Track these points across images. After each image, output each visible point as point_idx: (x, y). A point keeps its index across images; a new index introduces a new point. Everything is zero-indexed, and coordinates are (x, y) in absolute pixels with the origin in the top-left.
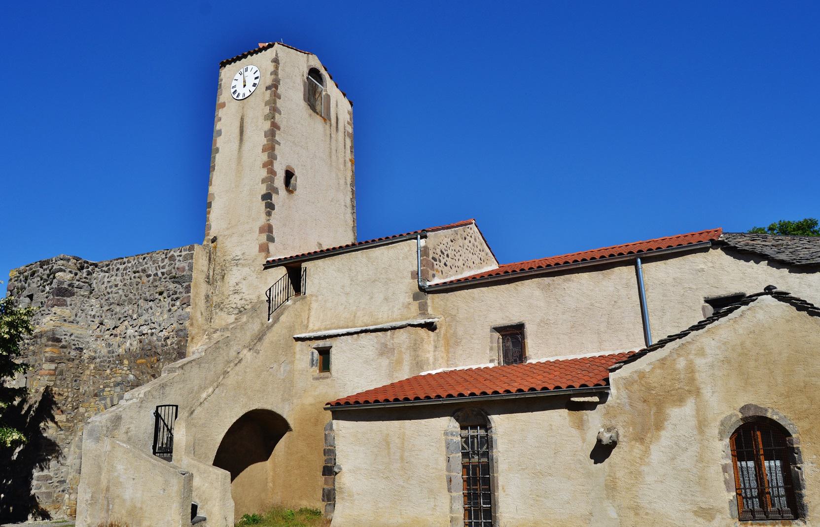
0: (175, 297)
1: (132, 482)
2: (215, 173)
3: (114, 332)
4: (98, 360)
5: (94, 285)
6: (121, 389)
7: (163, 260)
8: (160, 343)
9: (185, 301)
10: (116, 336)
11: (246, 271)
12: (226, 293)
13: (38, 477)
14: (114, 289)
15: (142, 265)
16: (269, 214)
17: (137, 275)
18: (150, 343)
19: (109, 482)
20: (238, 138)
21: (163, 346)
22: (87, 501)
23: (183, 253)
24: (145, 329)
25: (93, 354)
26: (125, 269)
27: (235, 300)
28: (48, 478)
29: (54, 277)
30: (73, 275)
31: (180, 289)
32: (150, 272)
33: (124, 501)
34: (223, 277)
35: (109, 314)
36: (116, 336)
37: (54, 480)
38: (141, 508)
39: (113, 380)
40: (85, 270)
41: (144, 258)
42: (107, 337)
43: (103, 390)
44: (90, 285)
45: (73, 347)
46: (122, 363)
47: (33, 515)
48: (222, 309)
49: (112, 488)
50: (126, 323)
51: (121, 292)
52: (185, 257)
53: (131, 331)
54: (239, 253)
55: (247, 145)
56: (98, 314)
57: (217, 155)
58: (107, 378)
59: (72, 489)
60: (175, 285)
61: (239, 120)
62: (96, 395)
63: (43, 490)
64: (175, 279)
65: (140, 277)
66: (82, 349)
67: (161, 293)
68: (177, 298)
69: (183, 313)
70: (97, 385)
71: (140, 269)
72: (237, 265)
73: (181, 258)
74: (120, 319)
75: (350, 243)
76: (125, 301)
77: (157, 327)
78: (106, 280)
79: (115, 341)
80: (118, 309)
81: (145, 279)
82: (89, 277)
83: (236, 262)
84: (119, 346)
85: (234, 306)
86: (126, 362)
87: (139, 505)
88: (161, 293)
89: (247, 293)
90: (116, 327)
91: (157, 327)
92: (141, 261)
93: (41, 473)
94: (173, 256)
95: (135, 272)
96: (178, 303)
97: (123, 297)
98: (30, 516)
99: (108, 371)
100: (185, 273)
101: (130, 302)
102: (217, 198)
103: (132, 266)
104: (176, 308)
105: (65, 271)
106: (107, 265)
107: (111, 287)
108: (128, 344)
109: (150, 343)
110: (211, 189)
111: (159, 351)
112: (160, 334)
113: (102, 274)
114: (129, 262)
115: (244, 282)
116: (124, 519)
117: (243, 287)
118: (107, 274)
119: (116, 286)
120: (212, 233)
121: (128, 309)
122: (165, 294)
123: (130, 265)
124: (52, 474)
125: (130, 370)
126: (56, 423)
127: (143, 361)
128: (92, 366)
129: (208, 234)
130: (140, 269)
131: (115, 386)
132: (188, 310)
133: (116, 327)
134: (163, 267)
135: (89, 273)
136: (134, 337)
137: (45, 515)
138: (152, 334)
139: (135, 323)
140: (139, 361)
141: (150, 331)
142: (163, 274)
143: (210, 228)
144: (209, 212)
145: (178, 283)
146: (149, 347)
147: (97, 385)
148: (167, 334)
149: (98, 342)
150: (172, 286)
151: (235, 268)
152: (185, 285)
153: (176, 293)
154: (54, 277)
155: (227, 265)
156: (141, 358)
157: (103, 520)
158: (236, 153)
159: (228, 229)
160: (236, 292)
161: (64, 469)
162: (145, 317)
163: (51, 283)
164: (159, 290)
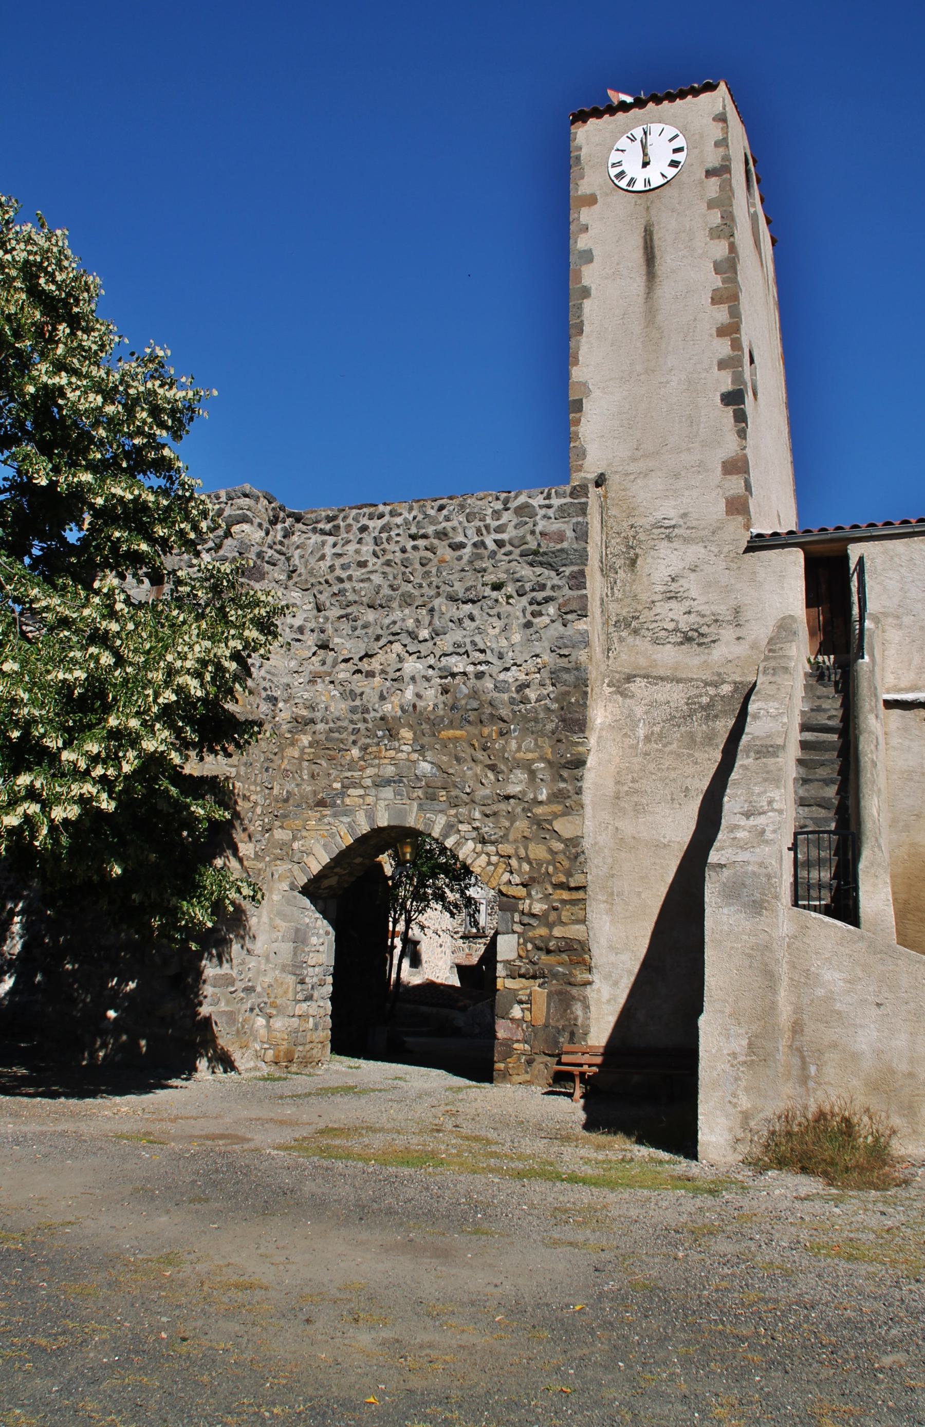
0: (540, 596)
1: (874, 1012)
2: (583, 339)
3: (365, 666)
4: (321, 727)
5: (296, 561)
6: (396, 793)
7: (497, 514)
8: (506, 697)
9: (574, 606)
10: (370, 674)
11: (694, 552)
12: (644, 597)
13: (215, 977)
14: (358, 573)
15: (434, 521)
16: (742, 434)
17: (421, 543)
18: (474, 694)
19: (798, 1010)
20: (643, 270)
21: (512, 701)
22: (734, 1055)
23: (556, 502)
24: (458, 664)
25: (305, 713)
26: (385, 528)
27: (673, 614)
28: (229, 981)
29: (228, 534)
30: (263, 534)
31: (550, 578)
32: (460, 538)
33: (855, 1057)
34: (633, 562)
35: (345, 626)
36: (370, 674)
37: (239, 985)
38: (911, 1075)
39: (369, 771)
40: (279, 526)
41: (441, 508)
42: (342, 676)
43: (343, 794)
44: (288, 559)
45: (264, 694)
46: (392, 735)
47: (210, 1060)
48: (636, 632)
49: (810, 1027)
50: (397, 647)
51: (377, 579)
52: (561, 508)
53: (412, 666)
54: (672, 513)
55: (666, 289)
56: (310, 625)
57: (587, 304)
58: (351, 766)
59: (273, 1005)
60: (539, 570)
61: (640, 232)
62: (321, 803)
63: (223, 1006)
64: (534, 557)
65: (432, 549)
66: (276, 699)
67: (497, 587)
68: (547, 600)
69: (569, 631)
70: (323, 782)
71: (430, 530)
72: (669, 538)
73: (551, 512)
74: (378, 638)
75: (783, 530)
76: (390, 599)
77: (494, 660)
78: (328, 551)
79: (371, 688)
80: (370, 616)
81: (448, 554)
82: (286, 541)
83: (668, 532)
84: (382, 698)
85: (671, 626)
86: (406, 734)
87: (903, 1067)
88: (497, 587)
89: (701, 599)
90: (367, 655)
91: (494, 660)
92: (432, 512)
93: (218, 971)
94: (526, 506)
95: (413, 537)
96: (552, 610)
97: (386, 591)
98: (202, 1064)
99: (355, 752)
100: (565, 545)
101: (407, 601)
102: (596, 393)
103: (407, 522)
104: (545, 620)
105: (252, 523)
106: (330, 519)
107: (344, 567)
108: (409, 693)
109: (474, 694)
110: (577, 374)
111: (504, 712)
112: (502, 676)
113: (316, 538)
114: (393, 514)
115: (693, 576)
116: (861, 1100)
117: (691, 585)
118: (331, 540)
119: (362, 564)
120: (591, 468)
121: (405, 617)
122: (510, 589)
123: (399, 520)
124: (234, 973)
125: (422, 750)
126: (241, 860)
127: (458, 733)
128: (305, 740)
129: (580, 468)
130: (430, 530)
131: (376, 785)
132: (581, 625)
133: (367, 655)
134: (500, 529)
135: (287, 534)
136: (427, 679)
137: (228, 1063)
138: (480, 676)
139: (424, 648)
140: (444, 734)
141: (470, 669)
142: (500, 544)
143: (583, 454)
144: (578, 422)
145: (550, 566)
146: (475, 704)
147: (323, 782)
148: (522, 677)
149: (320, 687)
150: (526, 571)
151: (665, 543)
152: (568, 570)
153: (543, 587)
154: (228, 534)
155: (641, 536)
156: (451, 726)
157: (790, 1104)
158: (641, 300)
159: (634, 460)
160: (671, 597)
161: (252, 963)
162: (456, 635)
163: (219, 547)
164: (491, 578)
